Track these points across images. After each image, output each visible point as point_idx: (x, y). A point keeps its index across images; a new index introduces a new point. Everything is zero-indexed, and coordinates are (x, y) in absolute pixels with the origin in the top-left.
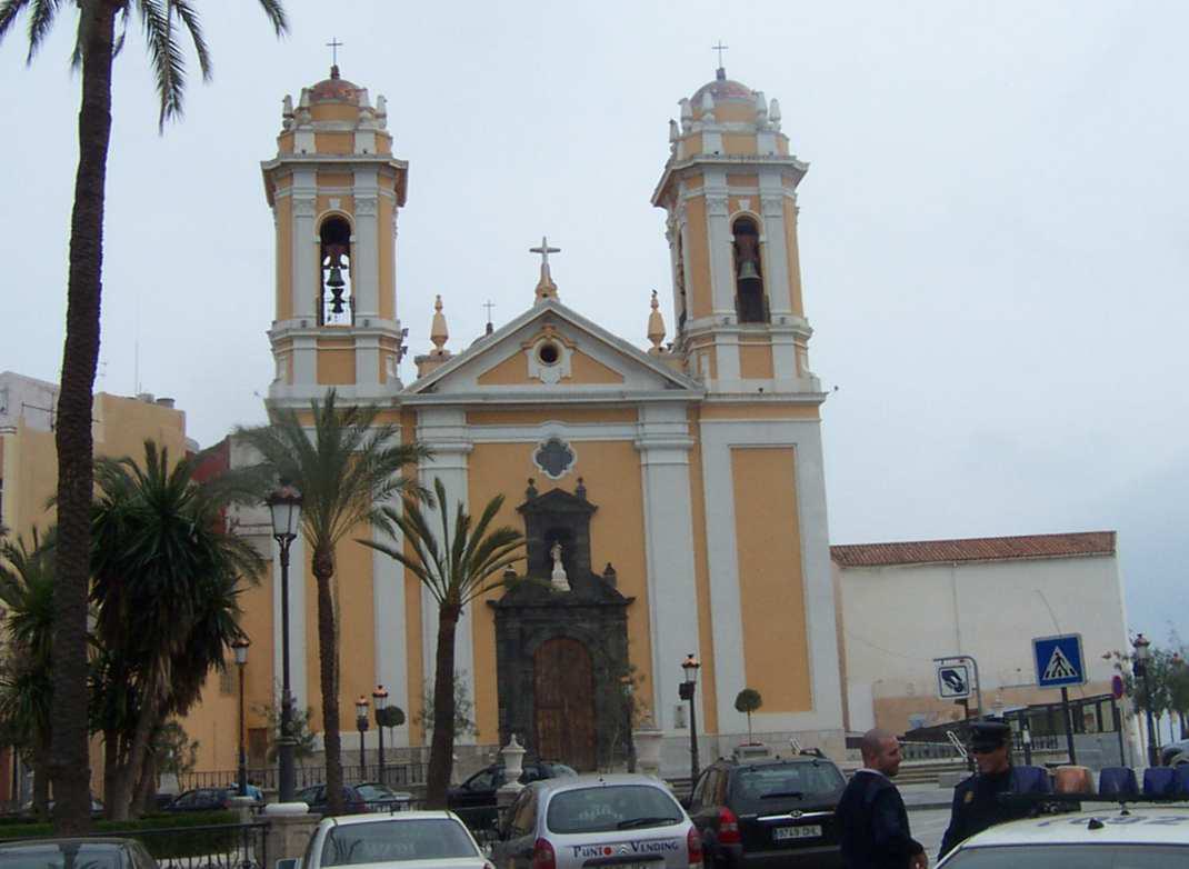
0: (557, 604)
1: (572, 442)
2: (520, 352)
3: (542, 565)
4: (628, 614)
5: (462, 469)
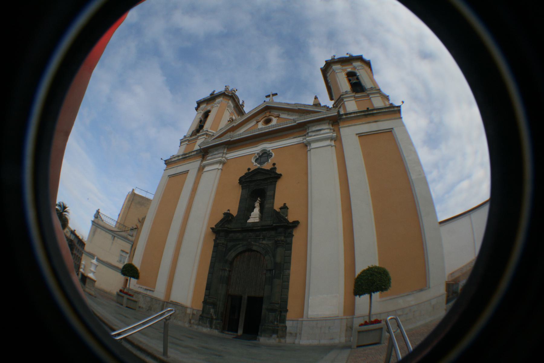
0: (253, 229)
1: (272, 149)
2: (256, 124)
3: (245, 210)
4: (294, 234)
5: (218, 169)
